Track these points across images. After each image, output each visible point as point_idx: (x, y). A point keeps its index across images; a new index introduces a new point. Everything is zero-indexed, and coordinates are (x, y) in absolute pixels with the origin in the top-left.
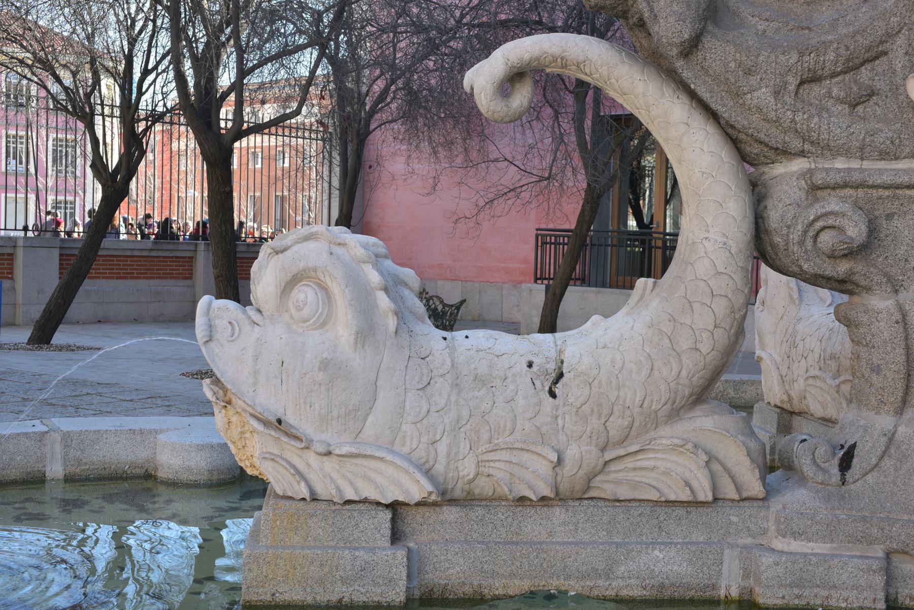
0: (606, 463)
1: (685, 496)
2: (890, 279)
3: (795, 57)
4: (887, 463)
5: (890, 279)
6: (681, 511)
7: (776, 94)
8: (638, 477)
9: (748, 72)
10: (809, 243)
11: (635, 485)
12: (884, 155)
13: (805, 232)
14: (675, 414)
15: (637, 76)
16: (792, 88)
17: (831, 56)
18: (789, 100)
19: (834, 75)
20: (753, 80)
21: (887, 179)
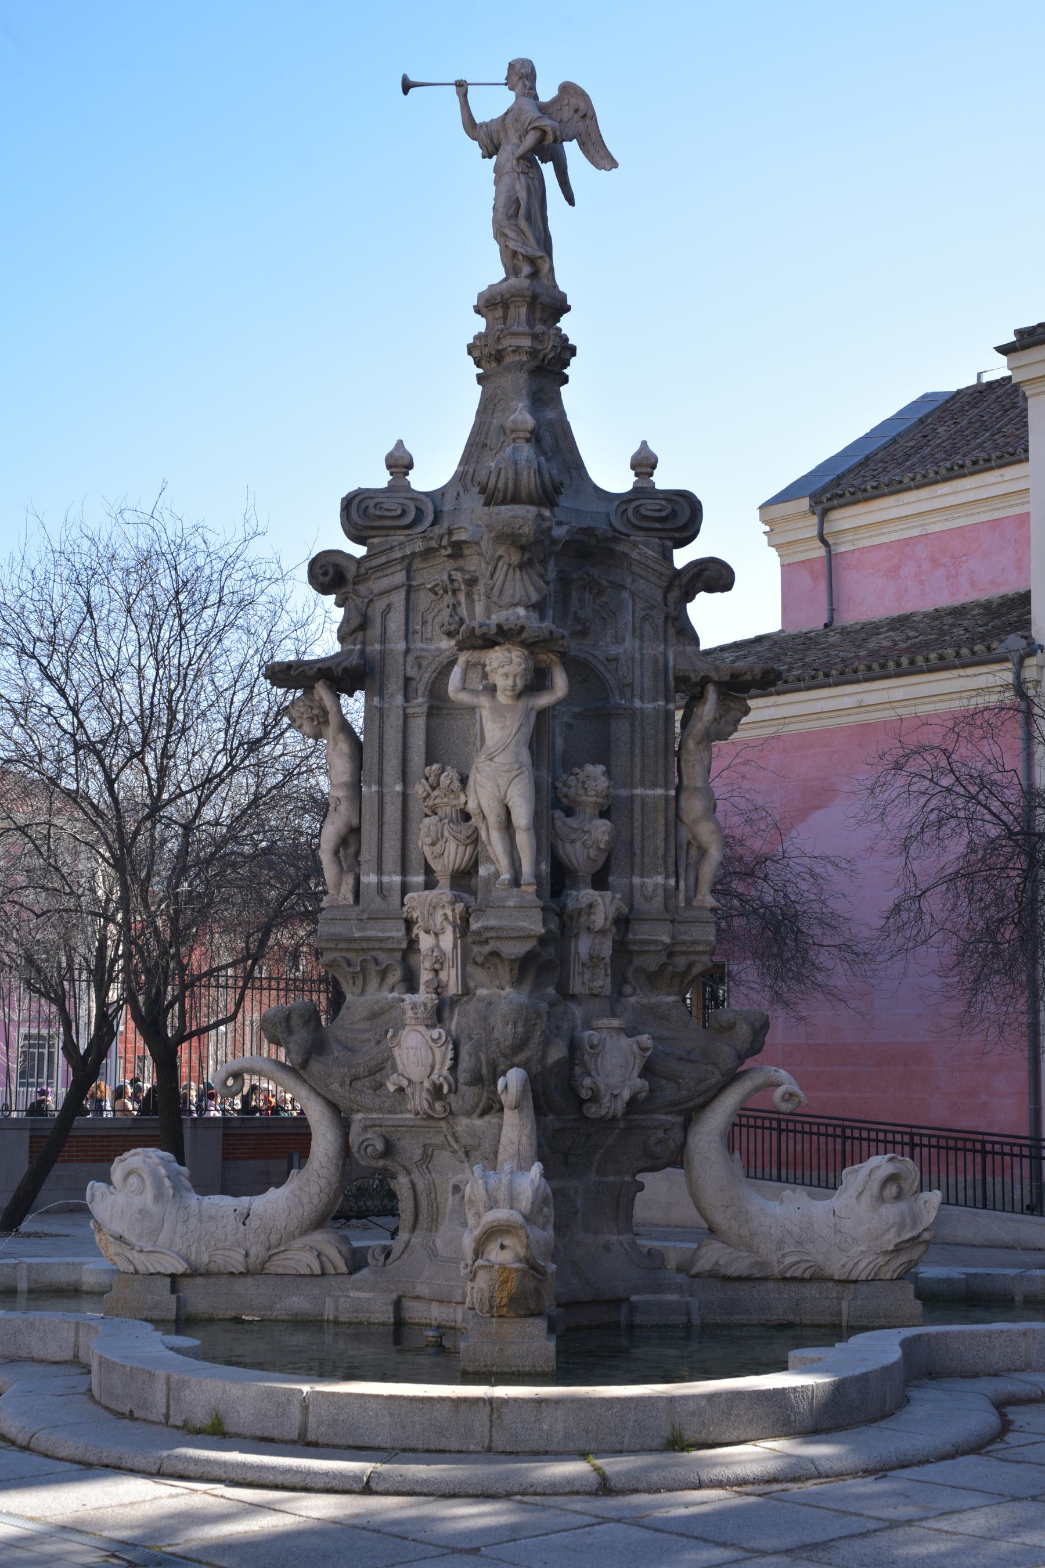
0: (270, 1257)
1: (308, 1272)
2: (405, 1168)
3: (346, 1070)
4: (405, 1256)
5: (405, 1168)
6: (308, 1279)
7: (341, 1085)
8: (287, 1263)
9: (329, 1076)
10: (362, 1152)
11: (285, 1267)
12: (390, 1112)
13: (359, 1147)
14: (304, 1233)
15: (285, 1077)
16: (348, 1082)
17: (361, 1069)
18: (347, 1088)
19: (365, 1077)
20: (332, 1079)
21: (390, 1123)
